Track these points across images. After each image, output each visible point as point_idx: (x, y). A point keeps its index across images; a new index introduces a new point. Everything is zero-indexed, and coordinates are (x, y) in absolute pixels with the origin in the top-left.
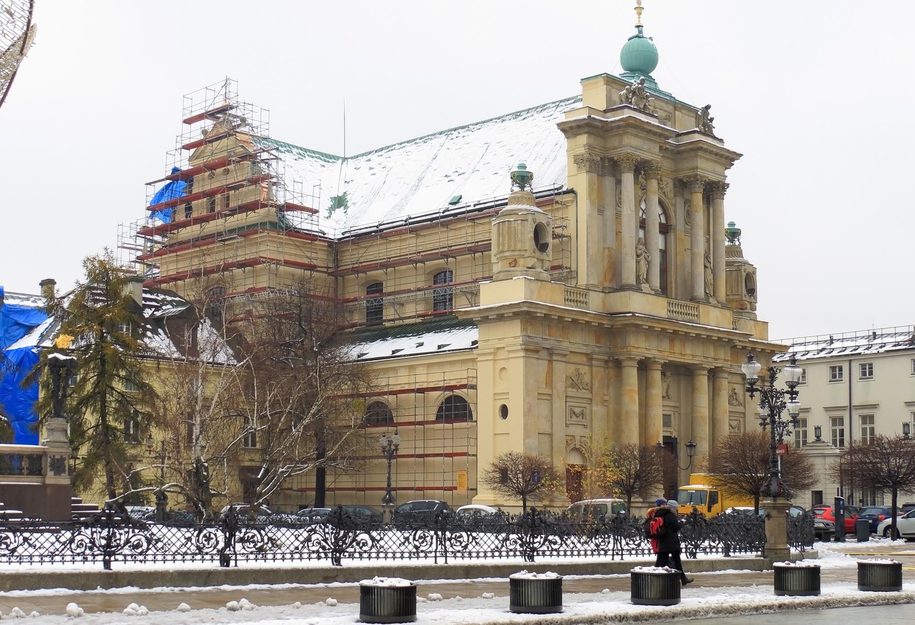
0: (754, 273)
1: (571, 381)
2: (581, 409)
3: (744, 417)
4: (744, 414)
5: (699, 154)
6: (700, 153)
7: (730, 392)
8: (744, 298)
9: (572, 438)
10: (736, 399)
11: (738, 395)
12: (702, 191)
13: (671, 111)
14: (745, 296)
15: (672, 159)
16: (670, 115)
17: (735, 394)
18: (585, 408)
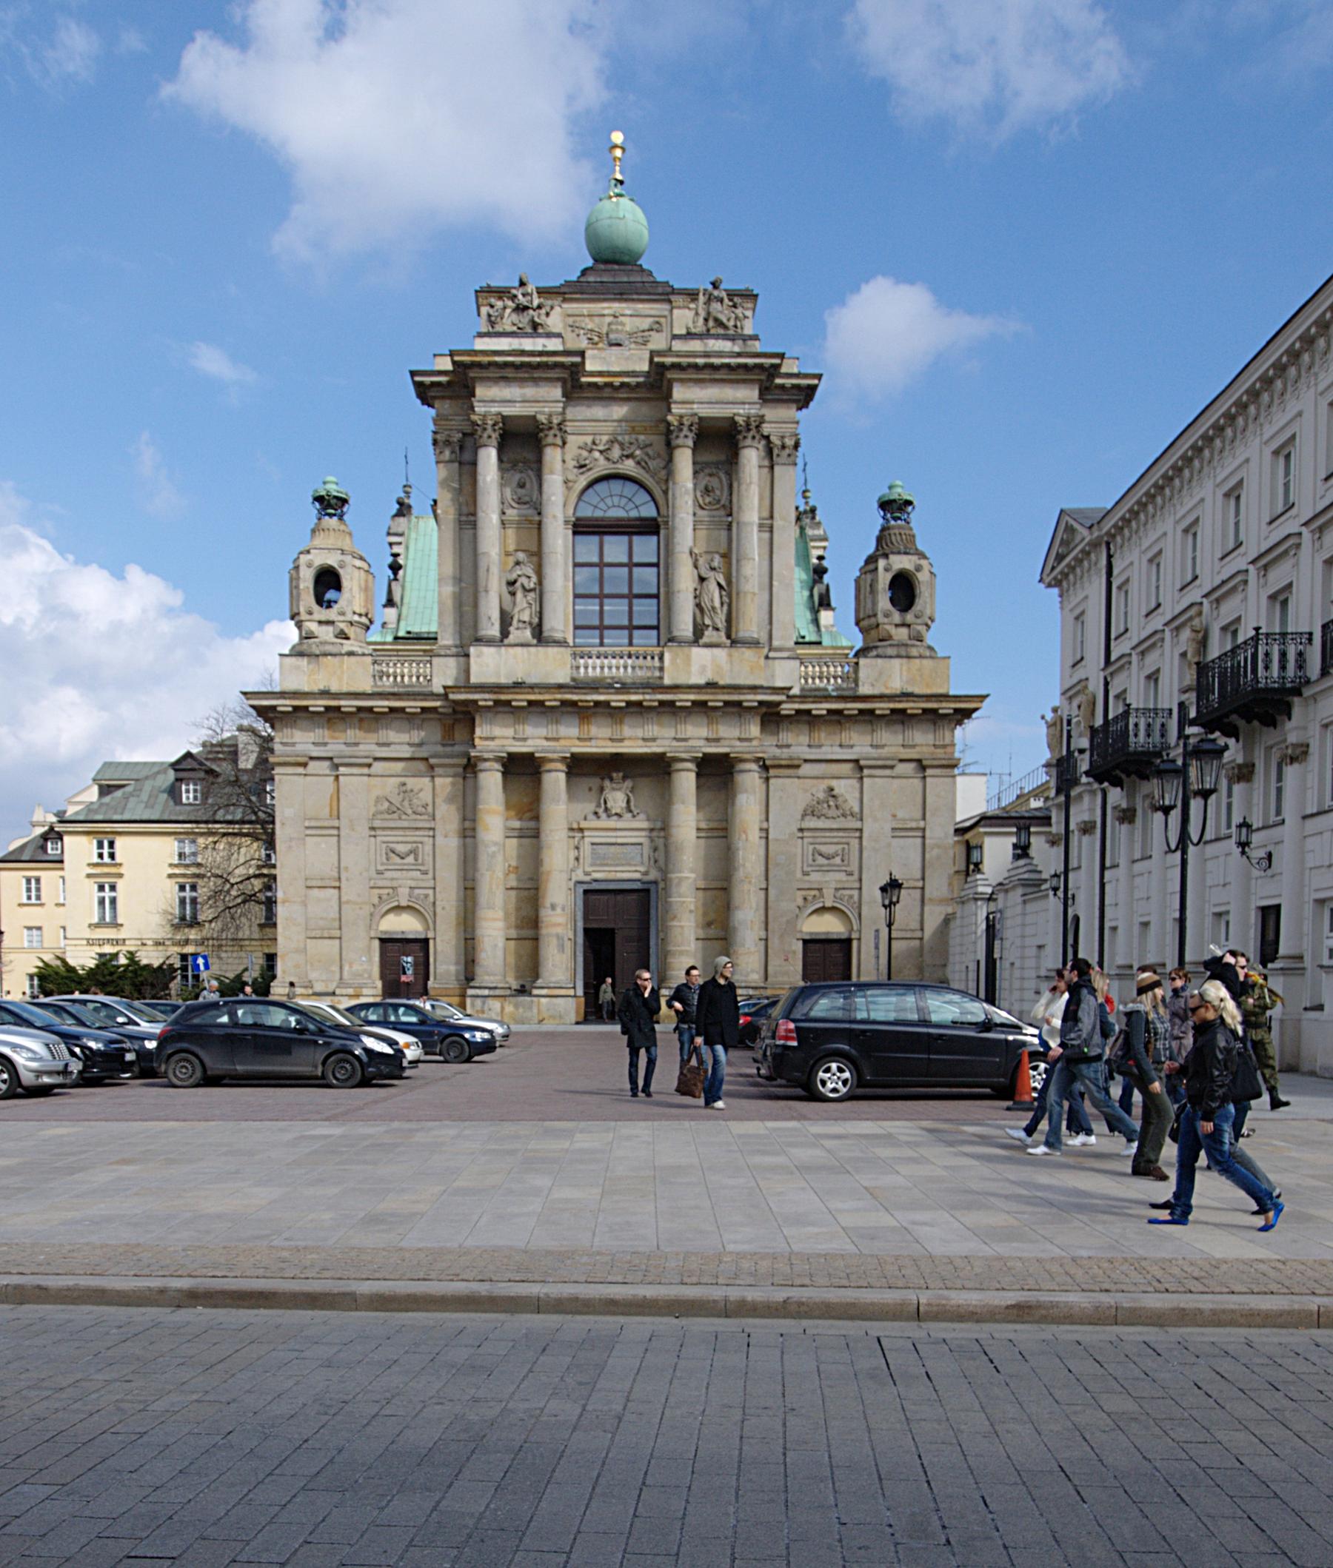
0: (919, 568)
1: (386, 805)
2: (414, 845)
3: (861, 838)
4: (861, 830)
5: (669, 376)
6: (669, 375)
7: (821, 795)
8: (881, 619)
9: (391, 891)
10: (837, 807)
11: (840, 799)
12: (690, 443)
13: (666, 313)
14: (887, 615)
15: (657, 399)
16: (662, 320)
17: (833, 796)
18: (421, 843)
